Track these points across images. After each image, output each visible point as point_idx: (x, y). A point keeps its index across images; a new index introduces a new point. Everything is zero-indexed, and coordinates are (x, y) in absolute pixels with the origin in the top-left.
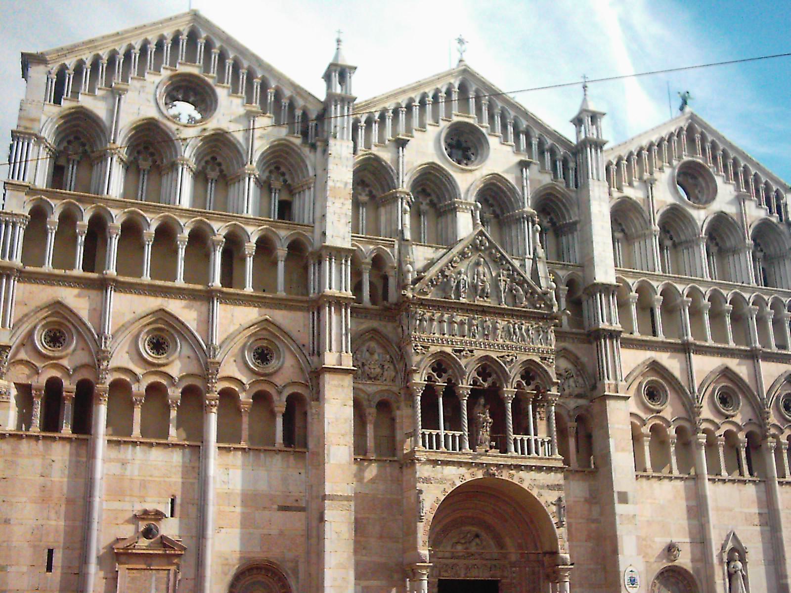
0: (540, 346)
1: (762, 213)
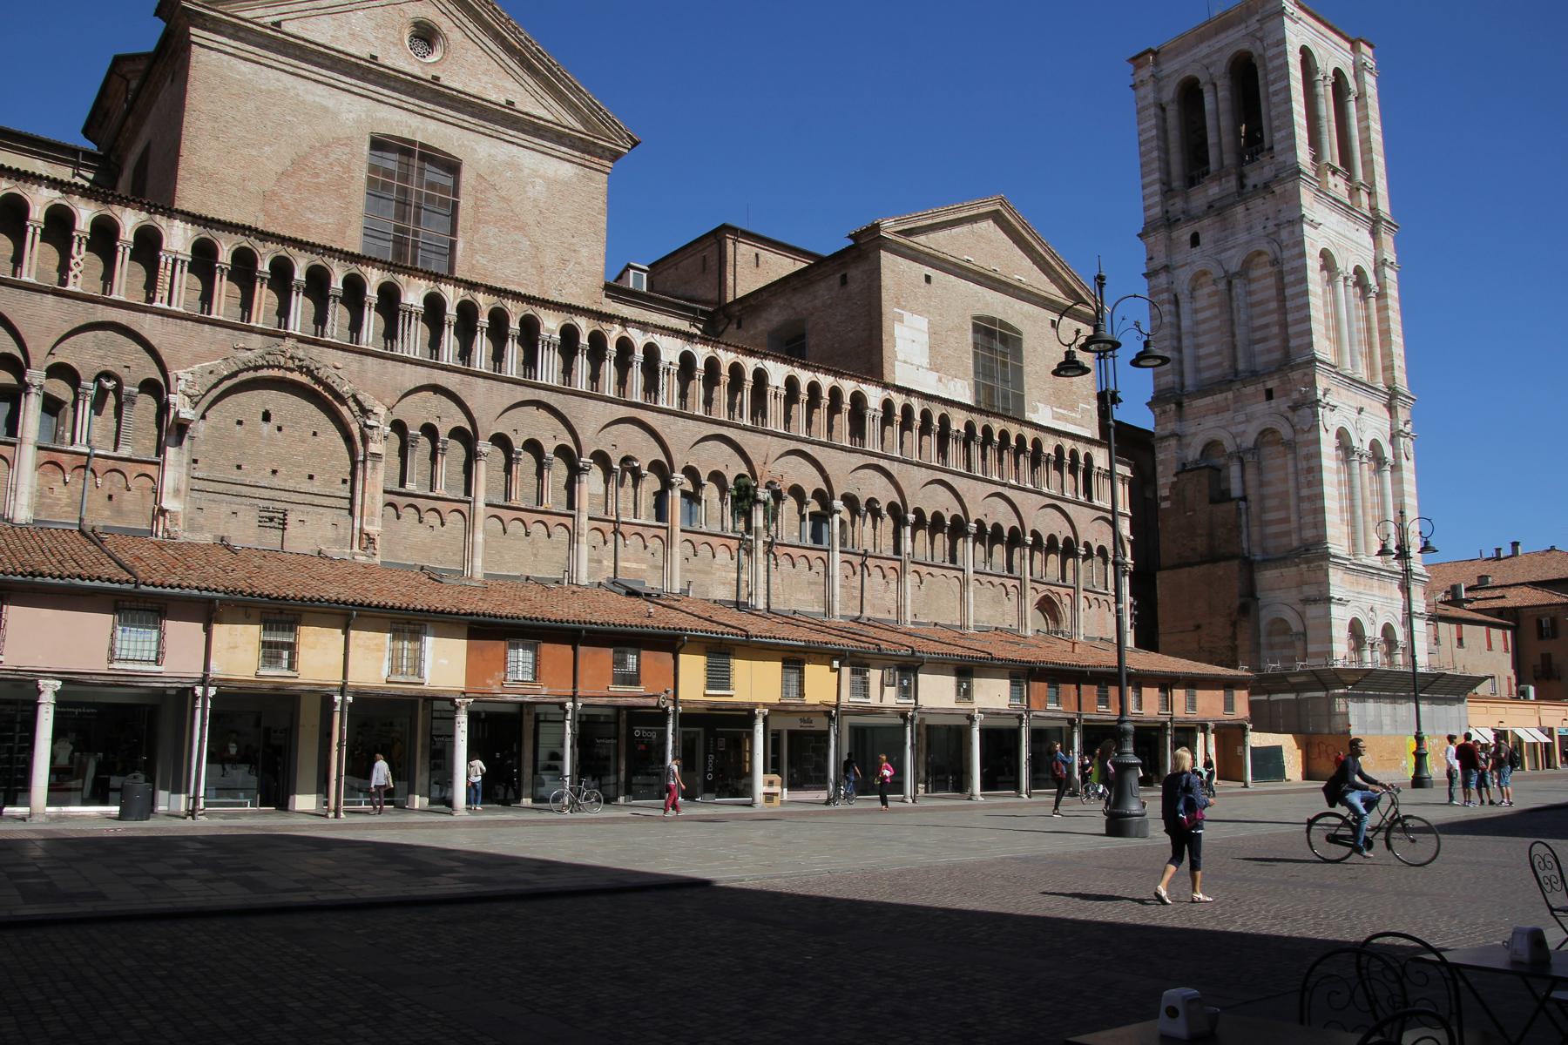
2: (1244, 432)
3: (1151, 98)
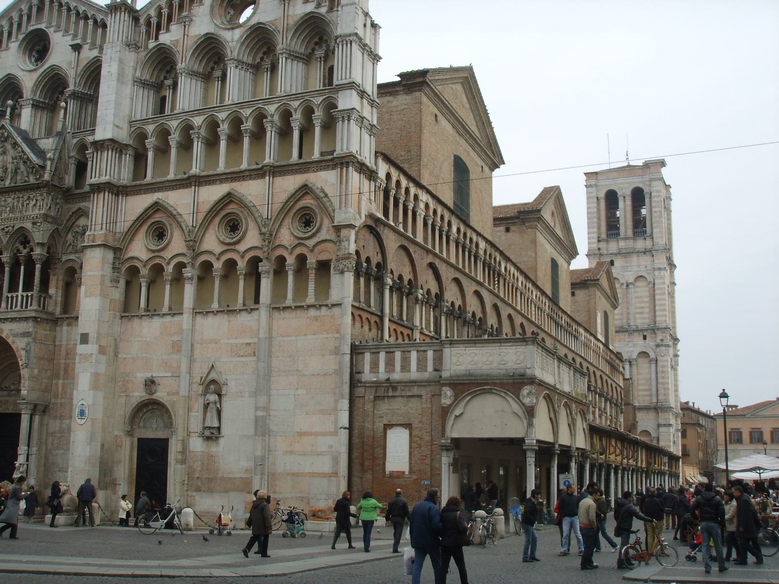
0: (27, 213)
1: (310, 7)
2: (632, 351)
3: (594, 194)
